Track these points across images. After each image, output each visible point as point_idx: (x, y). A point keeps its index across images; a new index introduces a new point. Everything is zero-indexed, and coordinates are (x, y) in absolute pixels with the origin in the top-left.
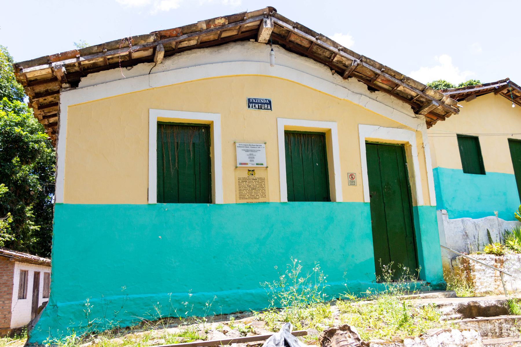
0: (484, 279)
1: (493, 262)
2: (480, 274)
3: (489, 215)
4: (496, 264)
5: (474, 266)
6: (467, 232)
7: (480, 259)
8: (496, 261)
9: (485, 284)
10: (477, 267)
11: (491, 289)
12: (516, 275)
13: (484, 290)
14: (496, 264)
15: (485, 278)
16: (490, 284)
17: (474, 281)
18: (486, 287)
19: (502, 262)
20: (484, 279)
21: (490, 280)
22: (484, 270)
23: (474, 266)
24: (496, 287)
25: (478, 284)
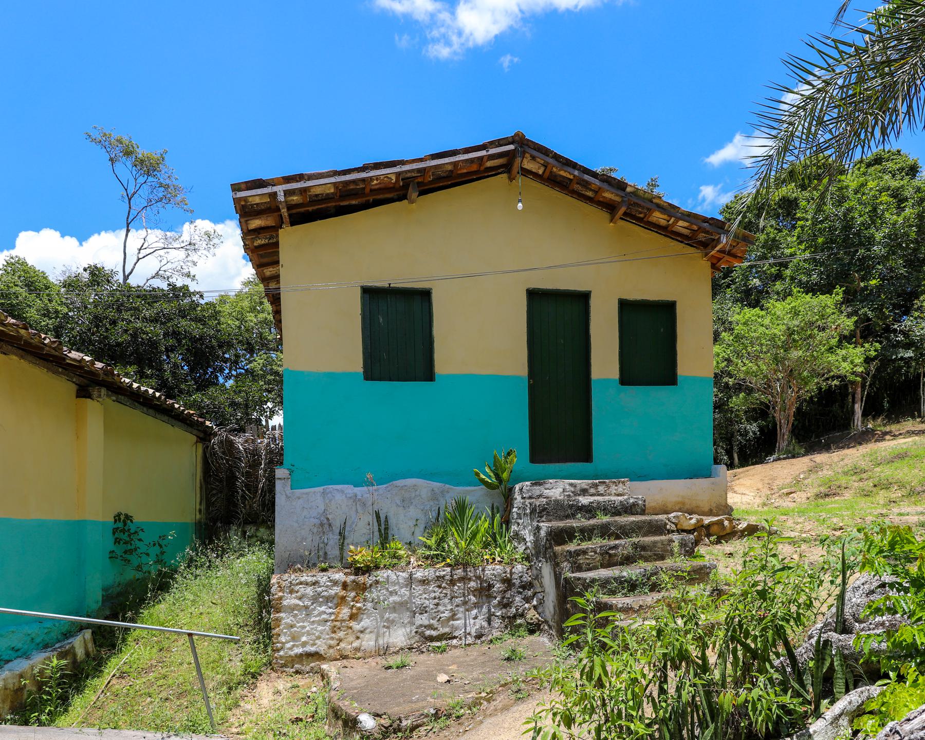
0: (304, 627)
1: (337, 590)
2: (295, 616)
3: (404, 477)
4: (343, 593)
5: (281, 598)
6: (330, 517)
7: (301, 583)
8: (345, 586)
9: (304, 639)
10: (290, 601)
11: (321, 647)
12: (393, 616)
13: (299, 650)
14: (343, 593)
15: (305, 624)
16: (319, 638)
17: (274, 632)
18: (304, 644)
19: (362, 588)
20: (304, 627)
21: (320, 628)
22: (306, 607)
23: (281, 598)
24: (333, 642)
25: (283, 639)
